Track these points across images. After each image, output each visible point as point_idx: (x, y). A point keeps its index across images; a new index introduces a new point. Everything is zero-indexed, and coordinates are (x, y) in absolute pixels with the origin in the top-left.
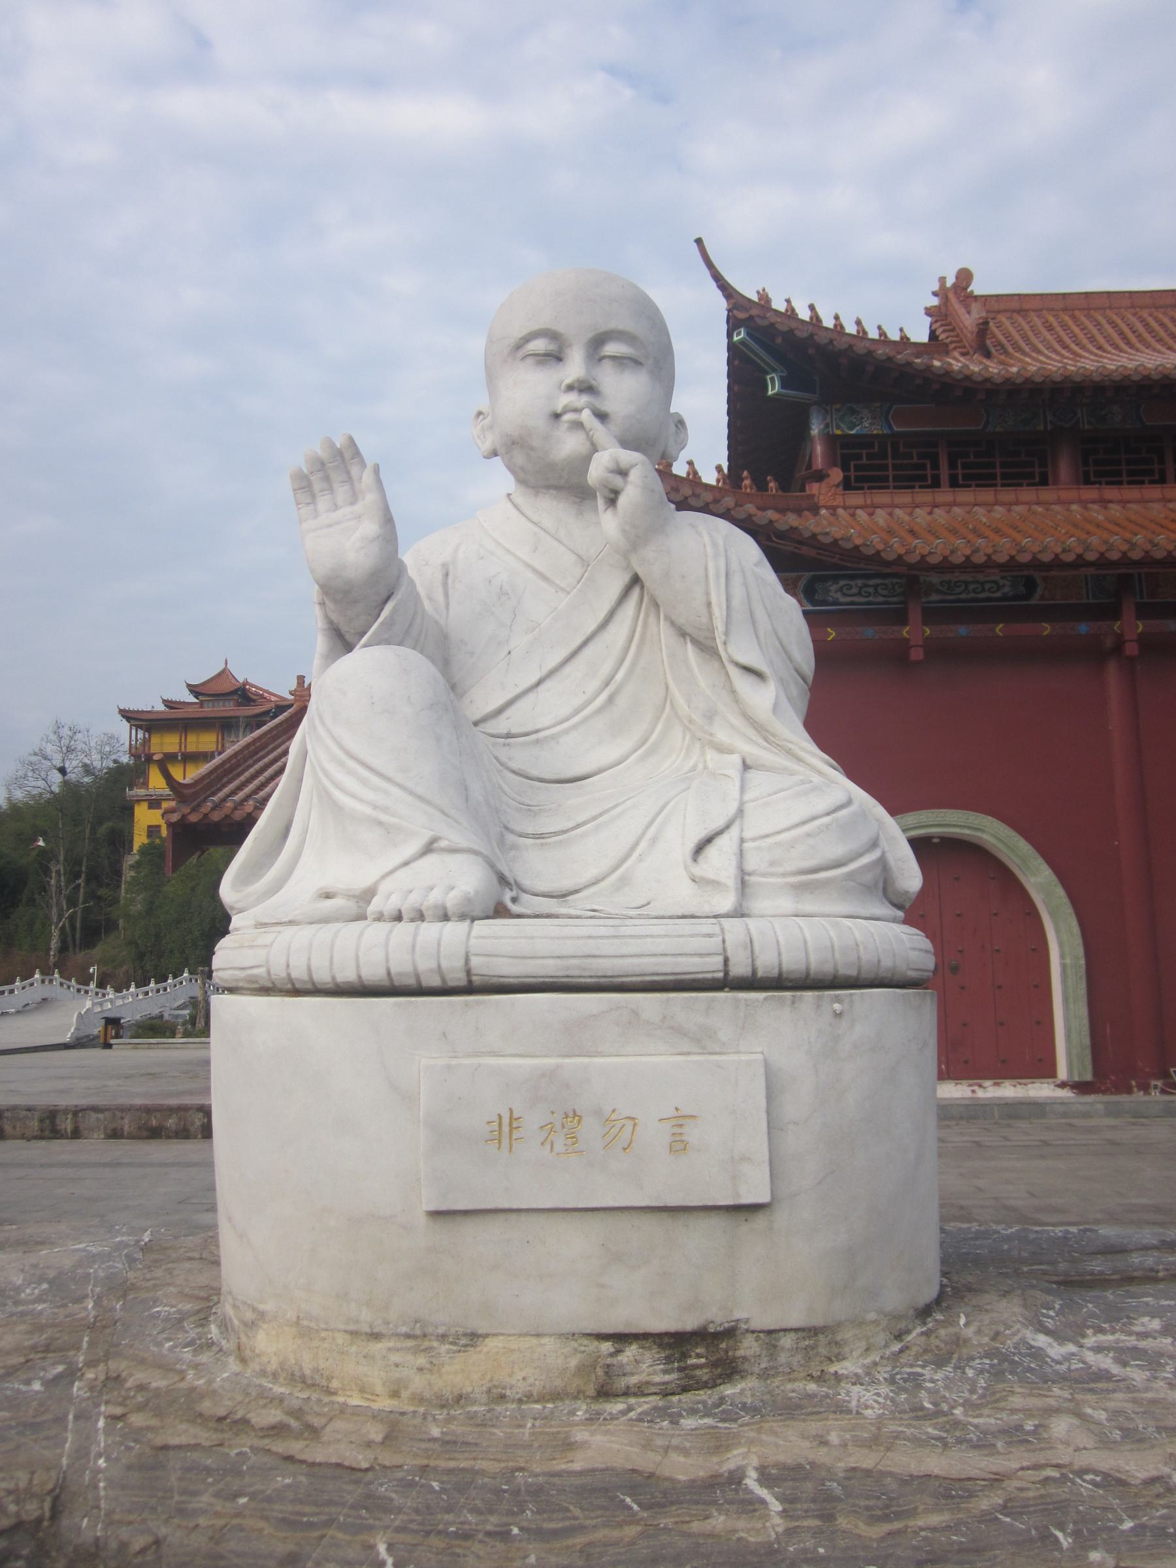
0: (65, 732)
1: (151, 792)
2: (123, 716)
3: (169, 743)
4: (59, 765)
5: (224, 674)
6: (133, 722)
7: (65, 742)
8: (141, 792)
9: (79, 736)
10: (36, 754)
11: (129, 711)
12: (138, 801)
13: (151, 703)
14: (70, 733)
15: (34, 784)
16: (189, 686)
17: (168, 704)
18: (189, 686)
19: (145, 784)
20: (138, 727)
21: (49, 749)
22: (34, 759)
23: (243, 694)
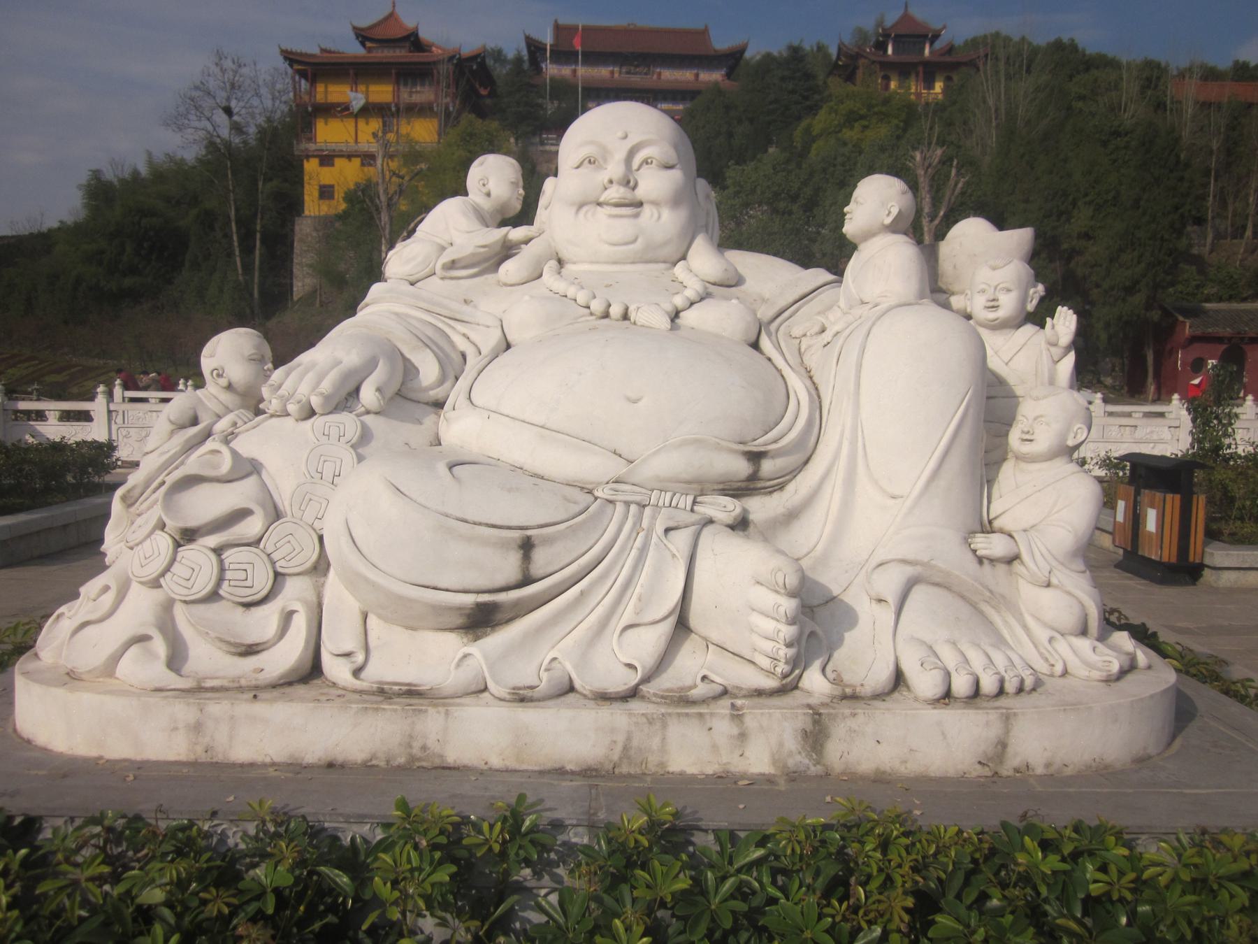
0: (228, 64)
1: (318, 146)
2: (286, 58)
3: (338, 92)
4: (224, 104)
5: (391, 15)
6: (296, 67)
7: (230, 75)
8: (312, 147)
9: (244, 71)
10: (197, 88)
11: (291, 53)
12: (308, 157)
13: (310, 48)
14: (234, 67)
15: (197, 124)
16: (355, 28)
17: (323, 50)
18: (355, 28)
19: (312, 139)
20: (303, 74)
21: (212, 84)
22: (196, 94)
23: (413, 41)
